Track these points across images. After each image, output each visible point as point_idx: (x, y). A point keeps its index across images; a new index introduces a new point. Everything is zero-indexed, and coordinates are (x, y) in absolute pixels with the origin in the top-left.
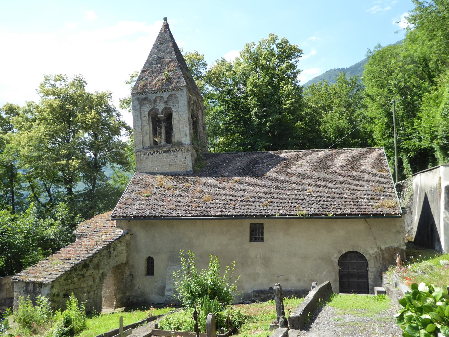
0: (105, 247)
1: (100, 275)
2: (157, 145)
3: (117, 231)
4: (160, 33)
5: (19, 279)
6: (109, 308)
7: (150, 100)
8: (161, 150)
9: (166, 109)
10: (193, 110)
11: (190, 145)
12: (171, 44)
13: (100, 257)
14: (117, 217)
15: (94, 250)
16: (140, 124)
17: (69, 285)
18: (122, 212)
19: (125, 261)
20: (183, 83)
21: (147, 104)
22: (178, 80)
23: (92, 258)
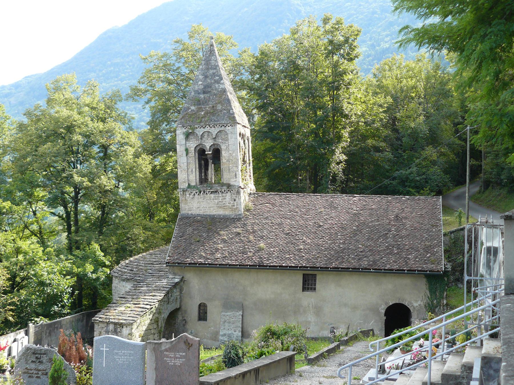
14: (171, 263)
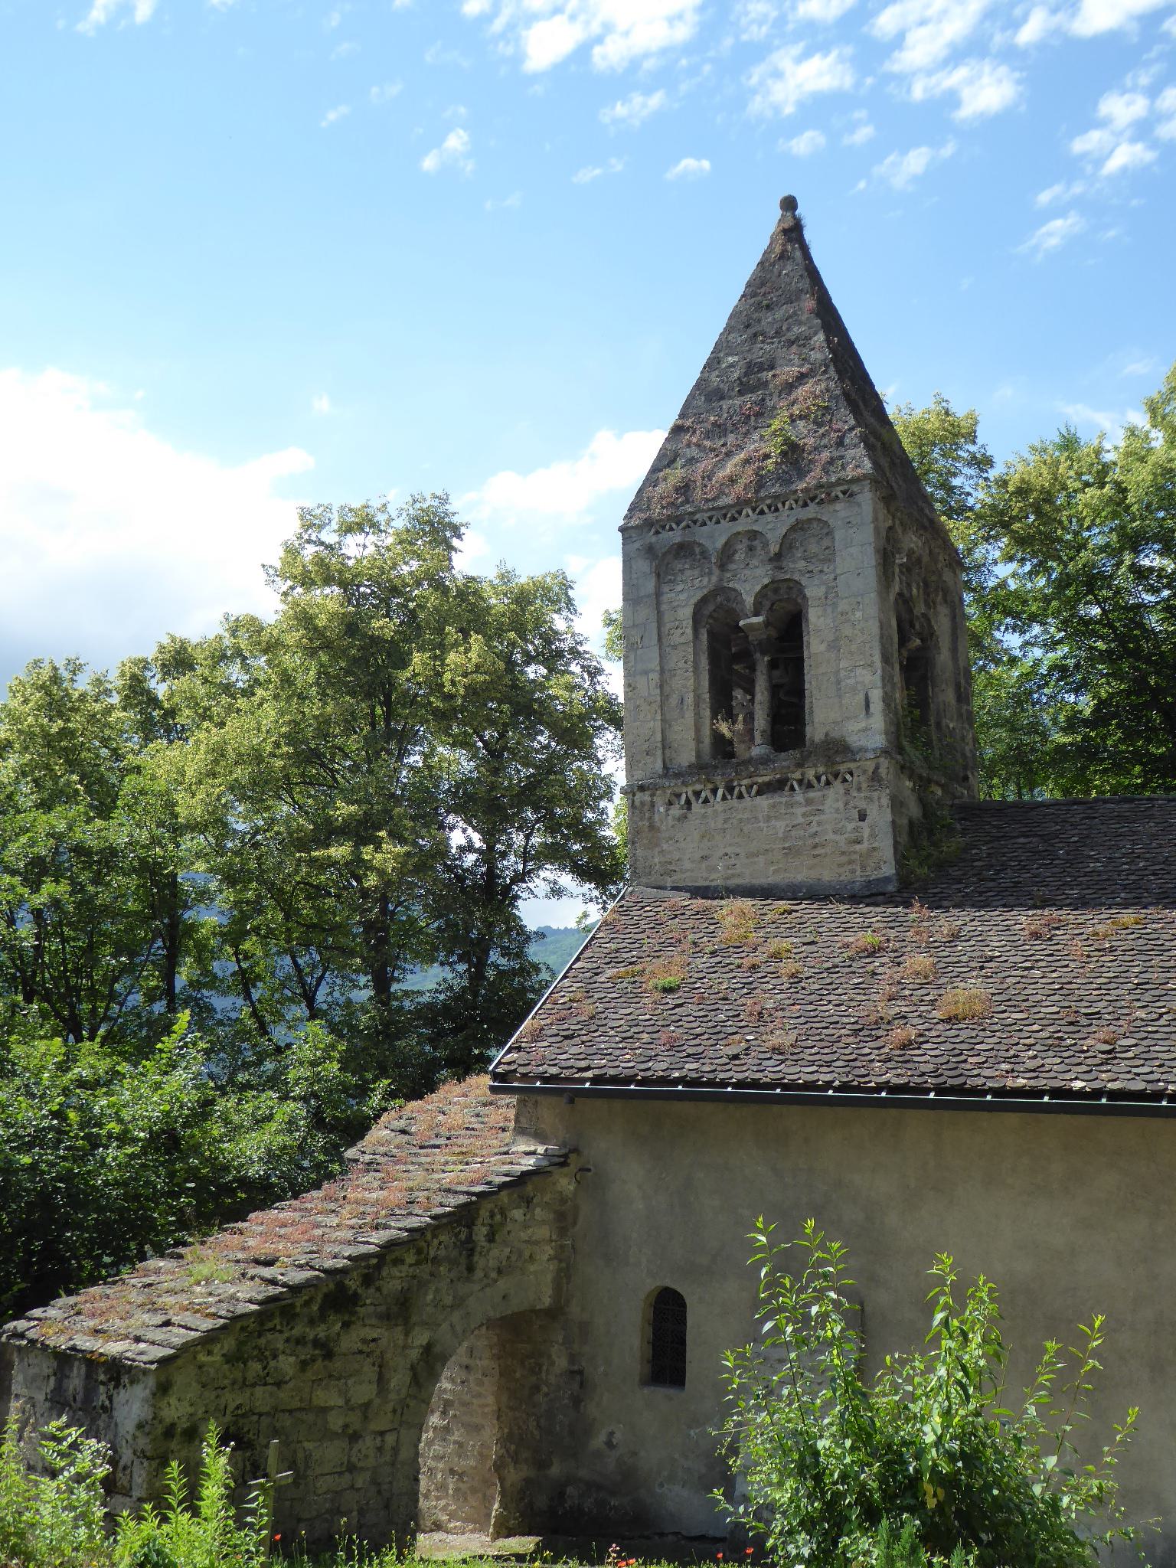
0: (444, 1215)
1: (414, 1354)
2: (731, 755)
3: (514, 1149)
4: (761, 263)
5: (31, 1334)
6: (472, 1531)
7: (704, 554)
8: (745, 782)
9: (776, 591)
10: (904, 601)
11: (885, 752)
12: (809, 303)
13: (418, 1263)
14: (519, 1080)
15: (390, 1227)
16: (655, 664)
17: (248, 1391)
18: (544, 1057)
19: (547, 1301)
20: (857, 467)
21: (688, 573)
22: (836, 454)
23: (378, 1267)
